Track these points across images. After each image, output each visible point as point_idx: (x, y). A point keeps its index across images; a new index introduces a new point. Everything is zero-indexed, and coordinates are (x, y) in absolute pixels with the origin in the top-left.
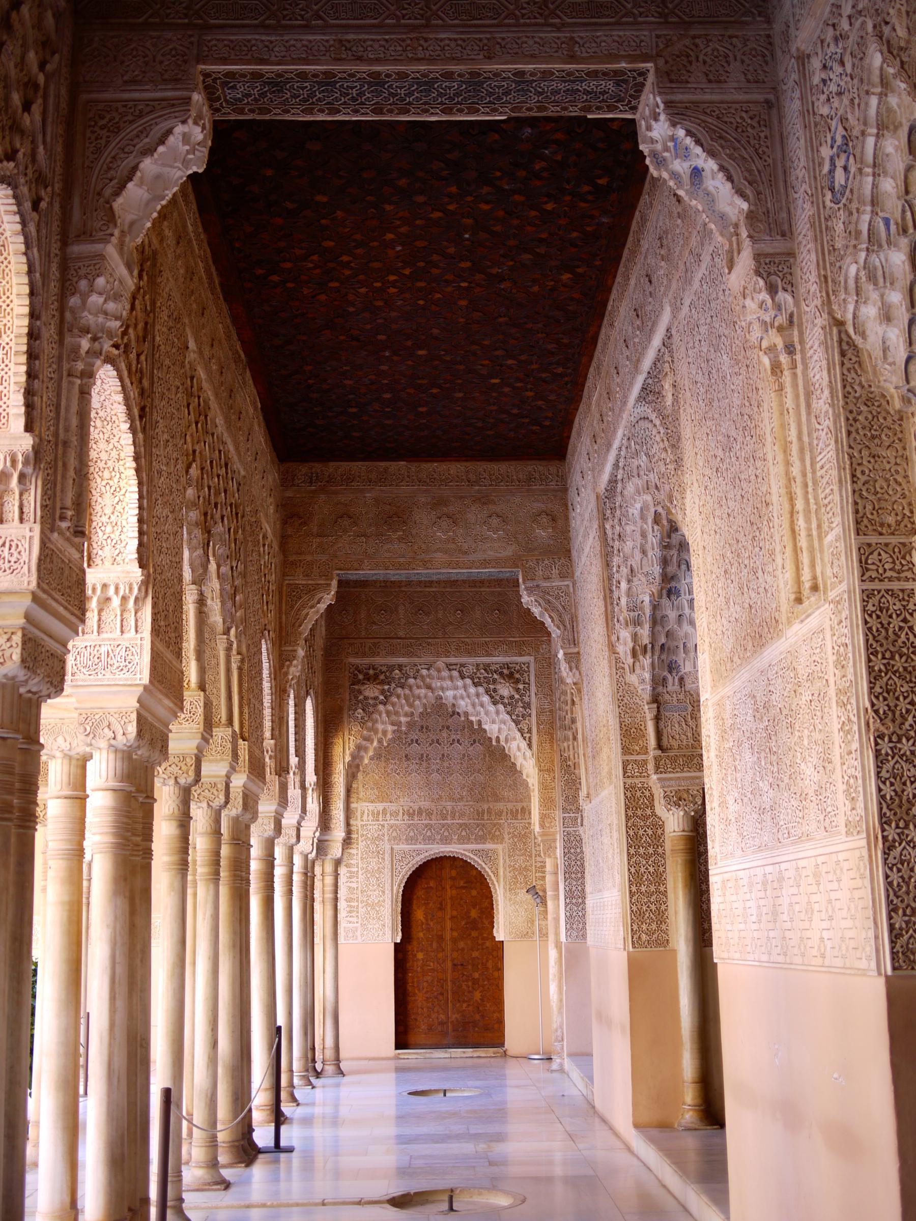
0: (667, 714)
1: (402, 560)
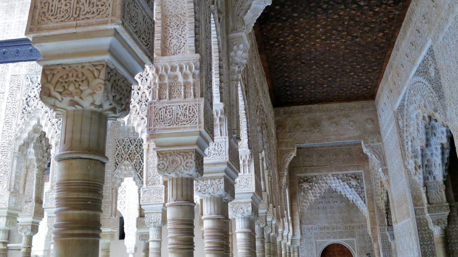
0: (430, 190)
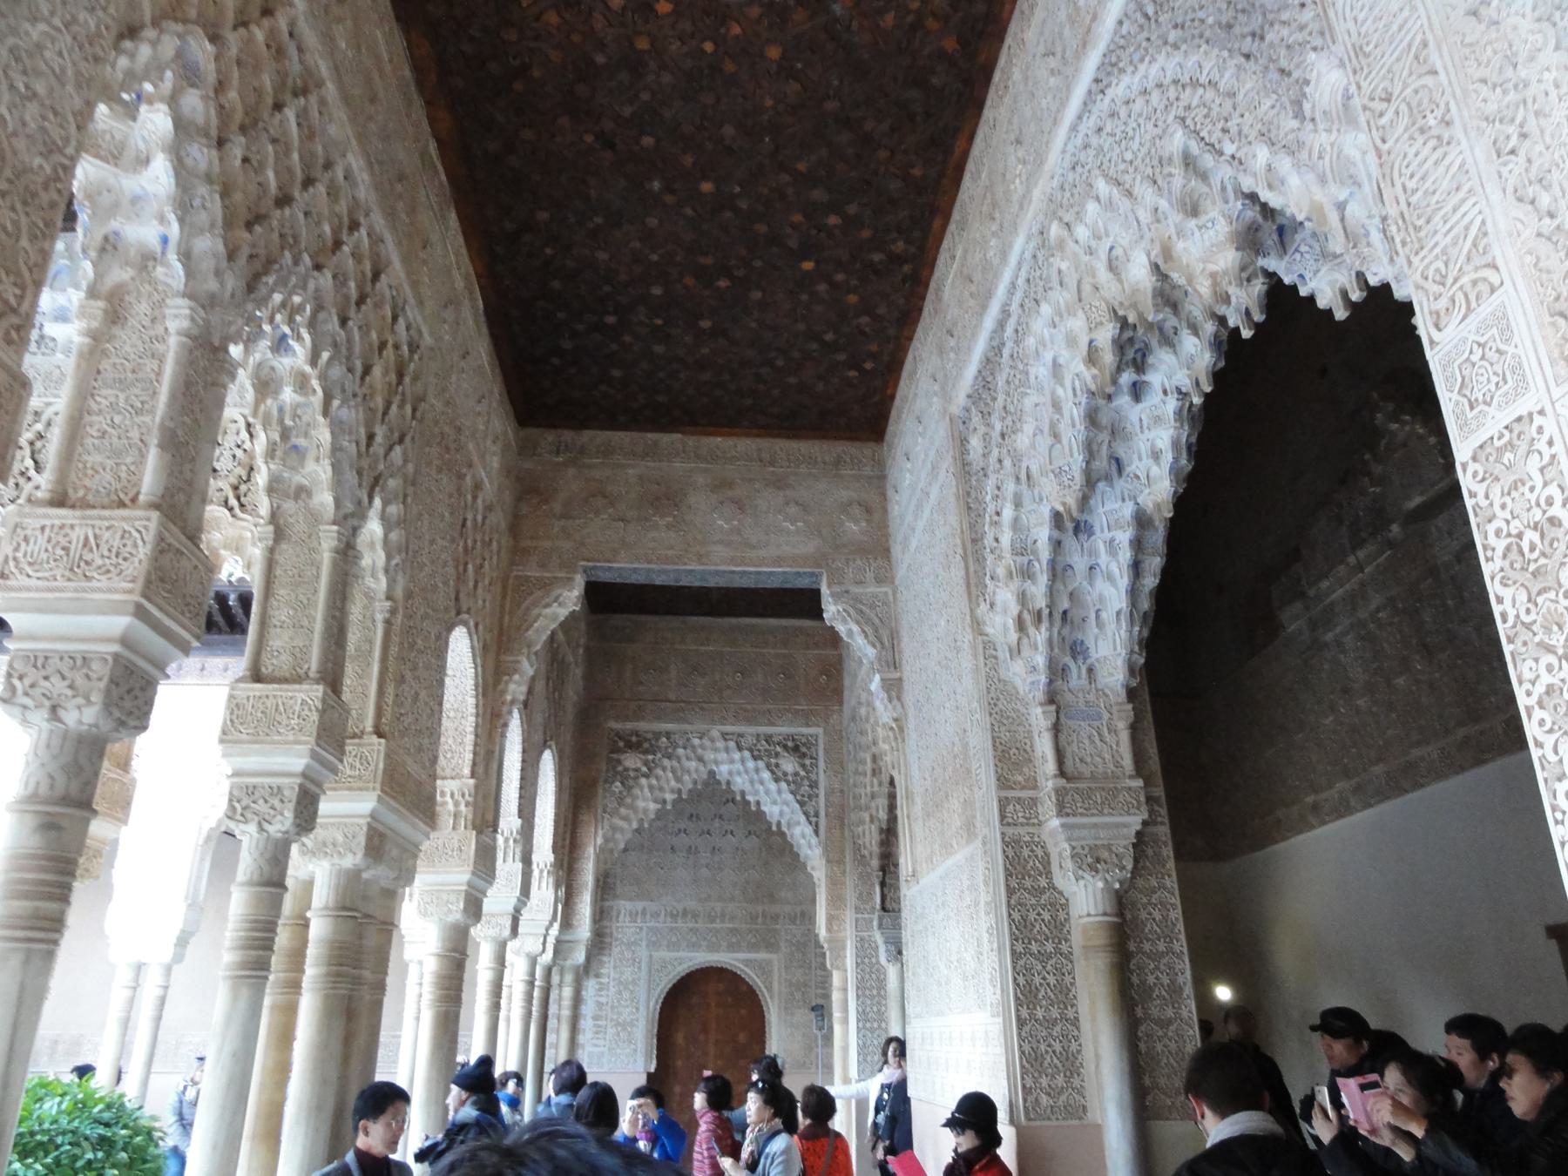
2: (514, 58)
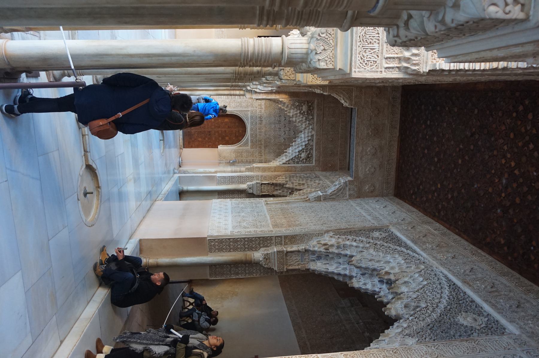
1: (360, 134)
2: (495, 113)
